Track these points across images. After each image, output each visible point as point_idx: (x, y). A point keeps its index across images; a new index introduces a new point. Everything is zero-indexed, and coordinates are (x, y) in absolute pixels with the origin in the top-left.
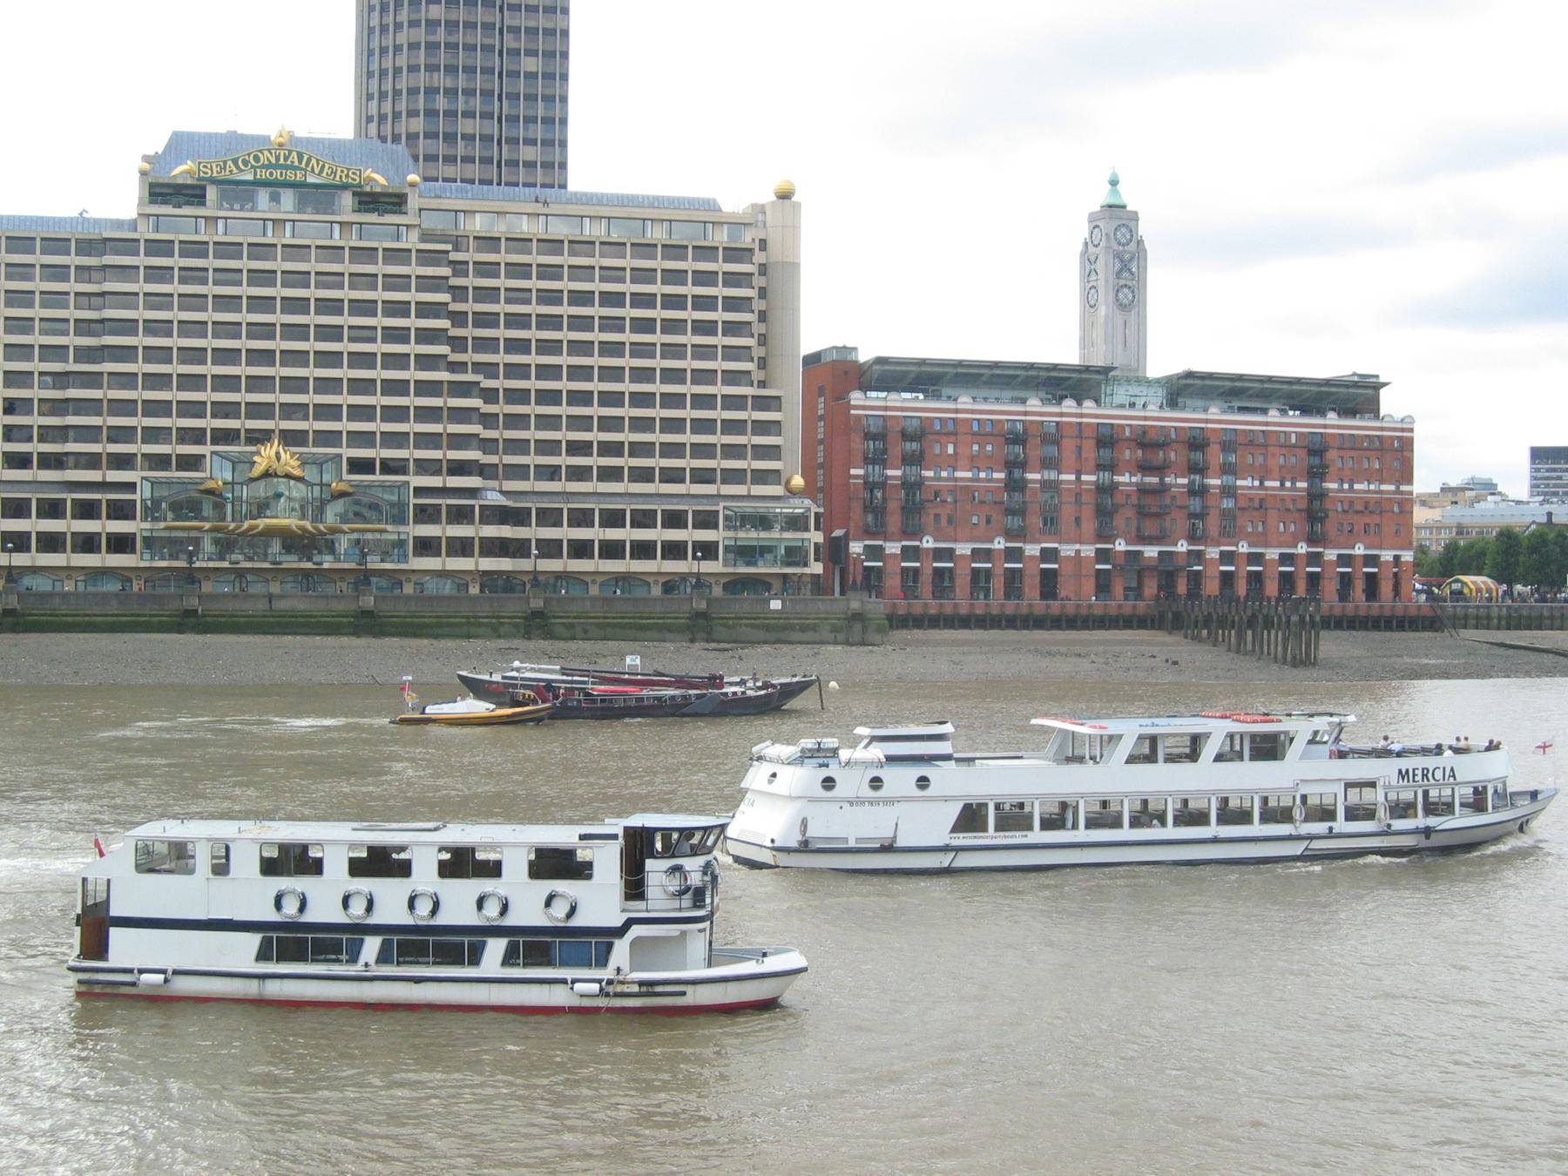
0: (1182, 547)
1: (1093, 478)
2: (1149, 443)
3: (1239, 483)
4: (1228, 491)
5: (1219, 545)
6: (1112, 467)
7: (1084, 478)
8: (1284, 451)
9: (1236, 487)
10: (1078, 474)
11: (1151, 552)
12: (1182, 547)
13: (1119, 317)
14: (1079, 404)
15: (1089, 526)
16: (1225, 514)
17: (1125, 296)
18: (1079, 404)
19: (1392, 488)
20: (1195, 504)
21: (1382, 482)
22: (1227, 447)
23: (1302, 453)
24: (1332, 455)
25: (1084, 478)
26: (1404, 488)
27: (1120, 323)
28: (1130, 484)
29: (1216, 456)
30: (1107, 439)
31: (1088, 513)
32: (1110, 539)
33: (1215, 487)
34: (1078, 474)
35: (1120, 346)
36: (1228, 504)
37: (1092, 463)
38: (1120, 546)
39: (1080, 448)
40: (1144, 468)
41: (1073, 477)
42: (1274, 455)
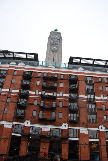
0: (65, 126)
1: (18, 91)
2: (50, 81)
3: (96, 98)
4: (92, 102)
5: (87, 126)
7: (14, 91)
11: (46, 128)
12: (65, 126)
13: (52, 54)
14: (17, 63)
15: (10, 112)
17: (55, 48)
18: (17, 63)
20: (73, 106)
22: (88, 83)
25: (14, 91)
27: (53, 55)
28: (38, 95)
29: (82, 86)
30: (27, 77)
31: (12, 106)
32: (21, 119)
37: (19, 85)
38: (28, 123)
40: (45, 89)
41: (8, 90)
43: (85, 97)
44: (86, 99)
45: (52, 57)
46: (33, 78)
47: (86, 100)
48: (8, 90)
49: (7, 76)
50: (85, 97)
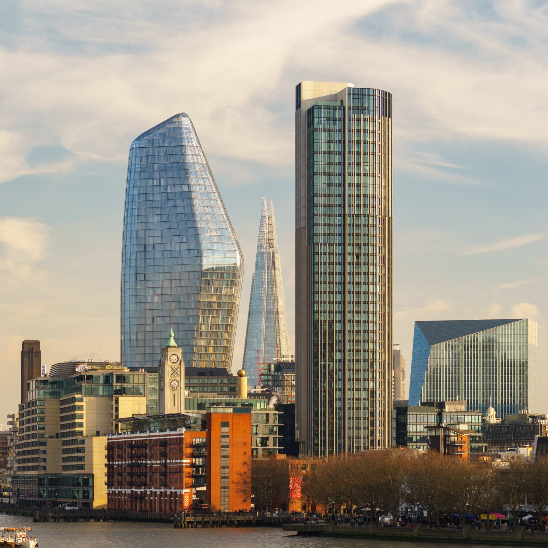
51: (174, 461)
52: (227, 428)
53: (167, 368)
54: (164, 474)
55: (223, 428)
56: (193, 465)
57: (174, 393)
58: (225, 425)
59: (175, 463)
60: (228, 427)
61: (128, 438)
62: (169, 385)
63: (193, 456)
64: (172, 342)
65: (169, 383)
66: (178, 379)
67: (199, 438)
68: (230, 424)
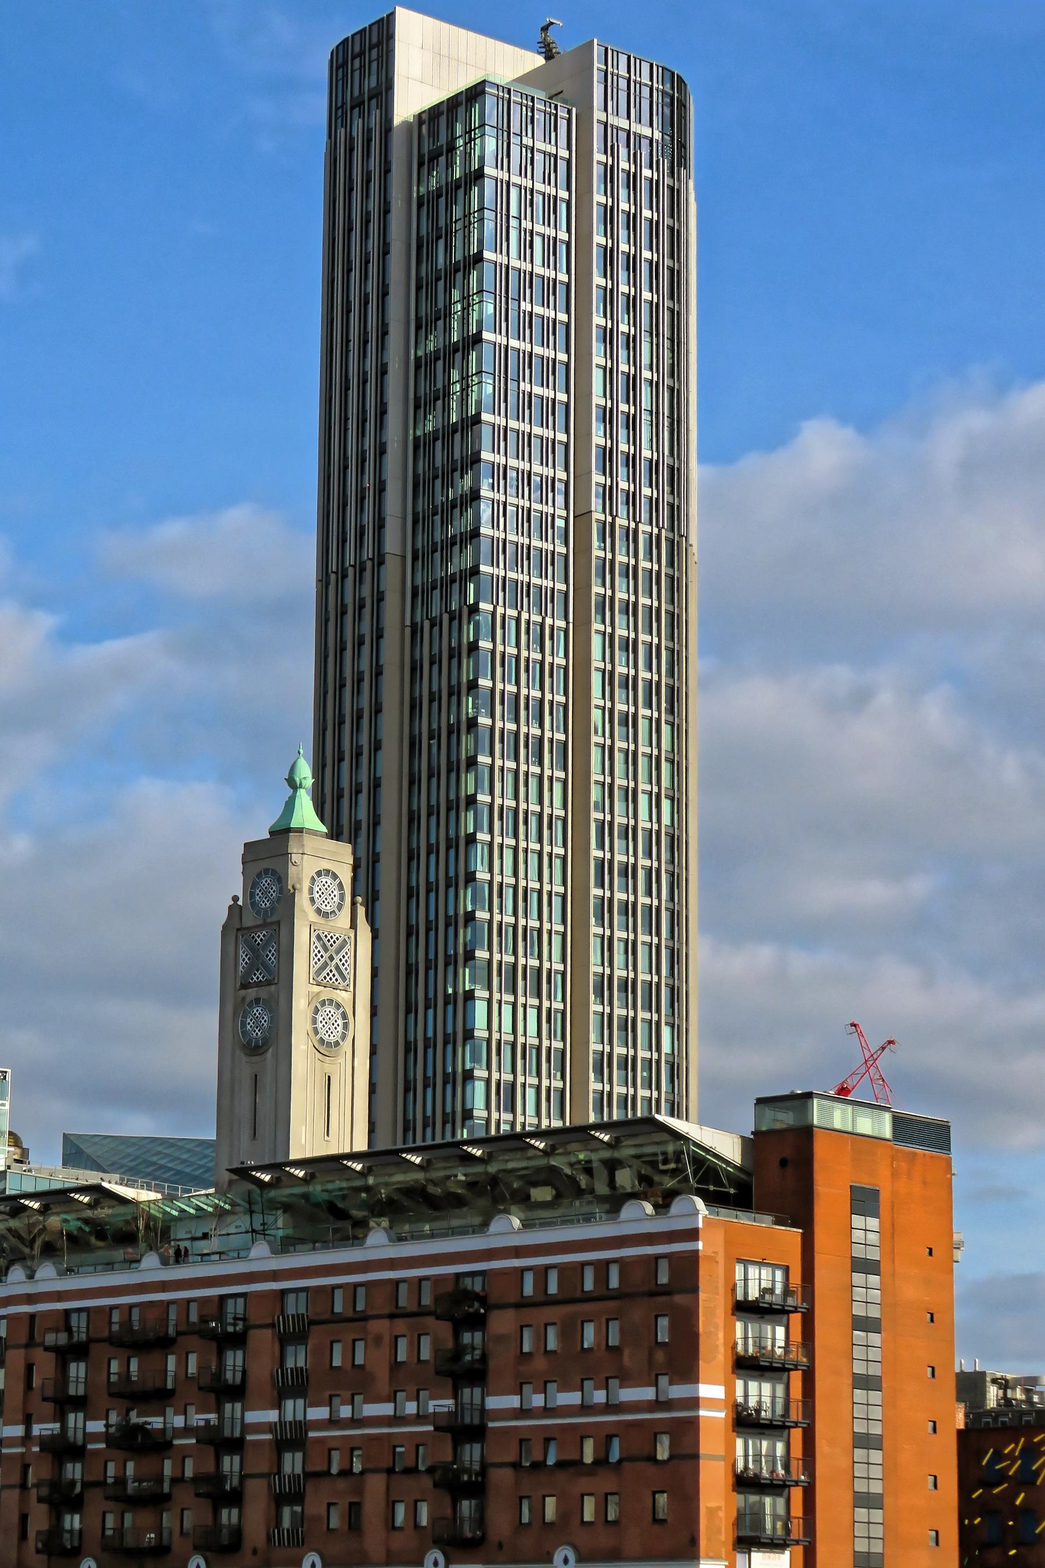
6: (64, 1403)
8: (401, 1326)
9: (302, 1427)
10: (28, 1421)
16: (288, 1495)
19: (648, 1393)
21: (626, 1379)
23: (444, 1329)
24: (501, 1322)
26: (677, 1392)
33: (258, 1428)
34: (28, 1421)
35: (246, 1133)
36: (293, 1463)
39: (29, 1368)
41: (18, 1431)
42: (378, 1340)
43: (272, 1416)
44: (270, 1427)
45: (244, 1102)
46: (94, 1348)
47: (269, 1437)
48: (18, 1431)
49: (8, 1352)
50: (272, 1416)
51: (573, 1398)
52: (873, 1223)
53: (302, 937)
54: (456, 1485)
55: (857, 1221)
56: (745, 1422)
57: (328, 1068)
58: (864, 1201)
59: (547, 1411)
60: (875, 1214)
61: (30, 1299)
62: (309, 1027)
63: (748, 1366)
64: (305, 814)
65: (310, 1014)
66: (343, 997)
67: (761, 1264)
68: (885, 1196)
